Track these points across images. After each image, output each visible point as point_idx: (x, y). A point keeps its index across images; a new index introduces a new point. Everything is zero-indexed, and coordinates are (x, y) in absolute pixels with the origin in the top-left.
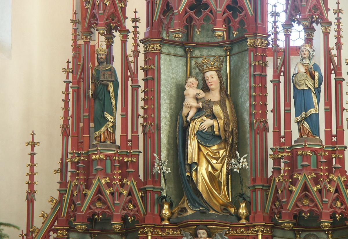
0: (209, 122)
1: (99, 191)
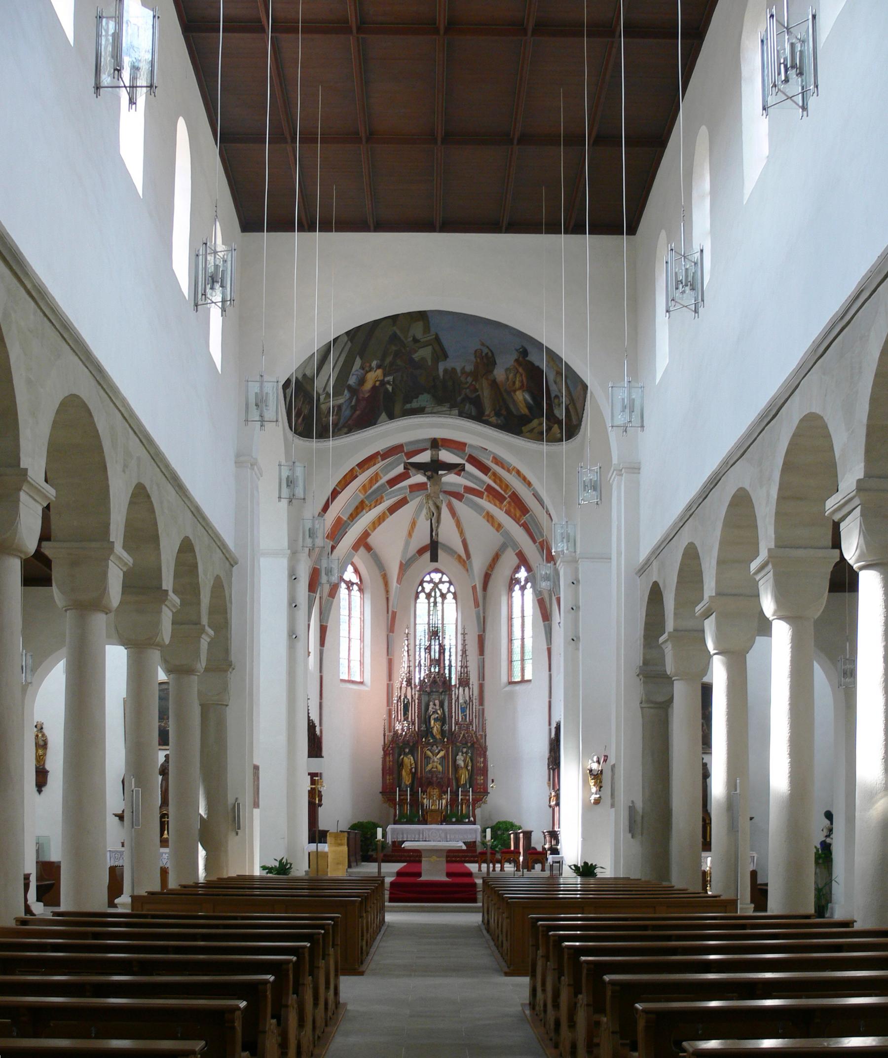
0: (437, 715)
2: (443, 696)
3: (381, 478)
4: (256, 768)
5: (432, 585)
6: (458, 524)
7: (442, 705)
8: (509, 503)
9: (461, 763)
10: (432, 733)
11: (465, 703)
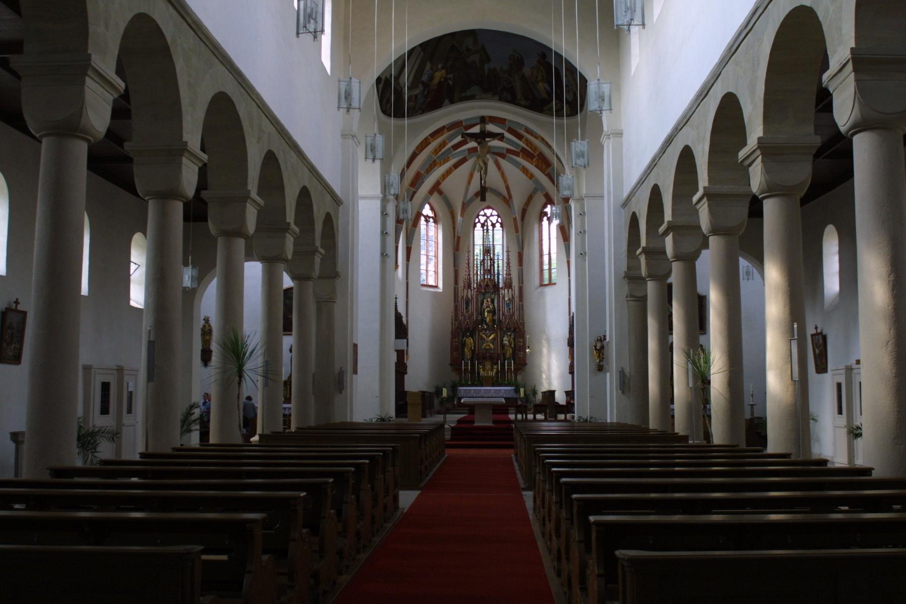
0: (489, 309)
1: (467, 323)
2: (493, 296)
3: (447, 144)
4: (355, 346)
5: (485, 218)
6: (503, 175)
7: (493, 301)
8: (537, 159)
9: (506, 342)
10: (485, 321)
11: (509, 299)
